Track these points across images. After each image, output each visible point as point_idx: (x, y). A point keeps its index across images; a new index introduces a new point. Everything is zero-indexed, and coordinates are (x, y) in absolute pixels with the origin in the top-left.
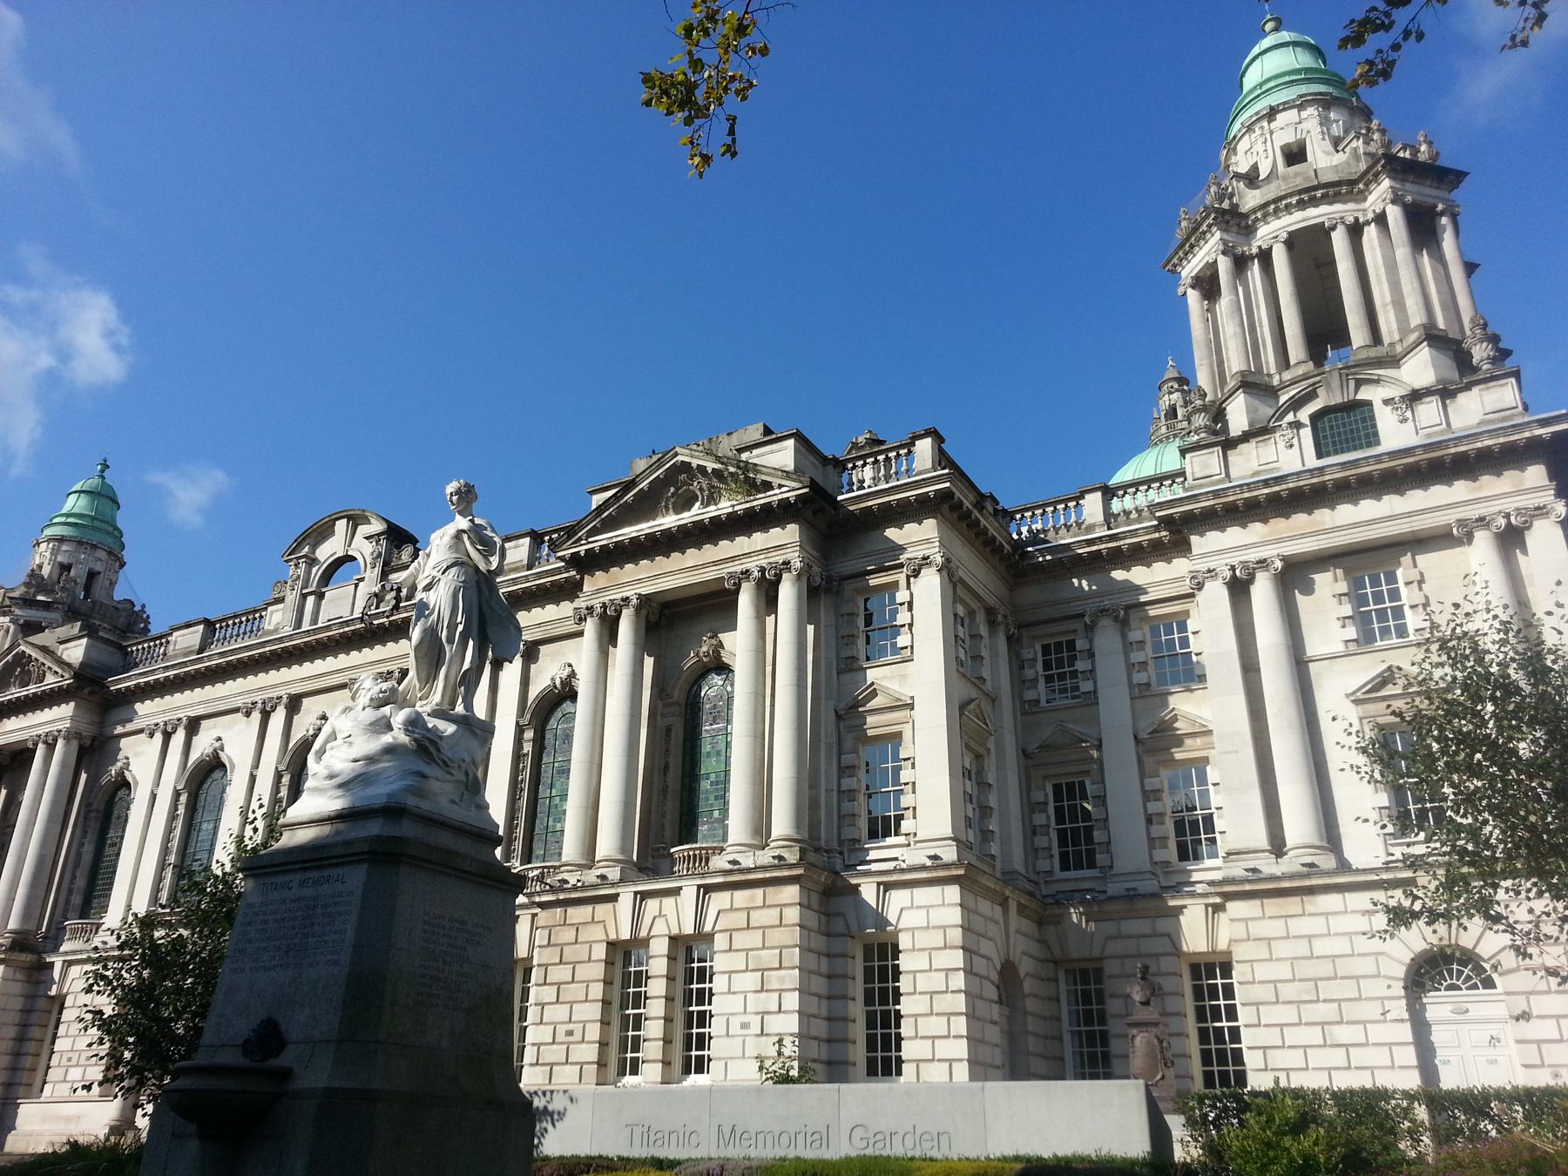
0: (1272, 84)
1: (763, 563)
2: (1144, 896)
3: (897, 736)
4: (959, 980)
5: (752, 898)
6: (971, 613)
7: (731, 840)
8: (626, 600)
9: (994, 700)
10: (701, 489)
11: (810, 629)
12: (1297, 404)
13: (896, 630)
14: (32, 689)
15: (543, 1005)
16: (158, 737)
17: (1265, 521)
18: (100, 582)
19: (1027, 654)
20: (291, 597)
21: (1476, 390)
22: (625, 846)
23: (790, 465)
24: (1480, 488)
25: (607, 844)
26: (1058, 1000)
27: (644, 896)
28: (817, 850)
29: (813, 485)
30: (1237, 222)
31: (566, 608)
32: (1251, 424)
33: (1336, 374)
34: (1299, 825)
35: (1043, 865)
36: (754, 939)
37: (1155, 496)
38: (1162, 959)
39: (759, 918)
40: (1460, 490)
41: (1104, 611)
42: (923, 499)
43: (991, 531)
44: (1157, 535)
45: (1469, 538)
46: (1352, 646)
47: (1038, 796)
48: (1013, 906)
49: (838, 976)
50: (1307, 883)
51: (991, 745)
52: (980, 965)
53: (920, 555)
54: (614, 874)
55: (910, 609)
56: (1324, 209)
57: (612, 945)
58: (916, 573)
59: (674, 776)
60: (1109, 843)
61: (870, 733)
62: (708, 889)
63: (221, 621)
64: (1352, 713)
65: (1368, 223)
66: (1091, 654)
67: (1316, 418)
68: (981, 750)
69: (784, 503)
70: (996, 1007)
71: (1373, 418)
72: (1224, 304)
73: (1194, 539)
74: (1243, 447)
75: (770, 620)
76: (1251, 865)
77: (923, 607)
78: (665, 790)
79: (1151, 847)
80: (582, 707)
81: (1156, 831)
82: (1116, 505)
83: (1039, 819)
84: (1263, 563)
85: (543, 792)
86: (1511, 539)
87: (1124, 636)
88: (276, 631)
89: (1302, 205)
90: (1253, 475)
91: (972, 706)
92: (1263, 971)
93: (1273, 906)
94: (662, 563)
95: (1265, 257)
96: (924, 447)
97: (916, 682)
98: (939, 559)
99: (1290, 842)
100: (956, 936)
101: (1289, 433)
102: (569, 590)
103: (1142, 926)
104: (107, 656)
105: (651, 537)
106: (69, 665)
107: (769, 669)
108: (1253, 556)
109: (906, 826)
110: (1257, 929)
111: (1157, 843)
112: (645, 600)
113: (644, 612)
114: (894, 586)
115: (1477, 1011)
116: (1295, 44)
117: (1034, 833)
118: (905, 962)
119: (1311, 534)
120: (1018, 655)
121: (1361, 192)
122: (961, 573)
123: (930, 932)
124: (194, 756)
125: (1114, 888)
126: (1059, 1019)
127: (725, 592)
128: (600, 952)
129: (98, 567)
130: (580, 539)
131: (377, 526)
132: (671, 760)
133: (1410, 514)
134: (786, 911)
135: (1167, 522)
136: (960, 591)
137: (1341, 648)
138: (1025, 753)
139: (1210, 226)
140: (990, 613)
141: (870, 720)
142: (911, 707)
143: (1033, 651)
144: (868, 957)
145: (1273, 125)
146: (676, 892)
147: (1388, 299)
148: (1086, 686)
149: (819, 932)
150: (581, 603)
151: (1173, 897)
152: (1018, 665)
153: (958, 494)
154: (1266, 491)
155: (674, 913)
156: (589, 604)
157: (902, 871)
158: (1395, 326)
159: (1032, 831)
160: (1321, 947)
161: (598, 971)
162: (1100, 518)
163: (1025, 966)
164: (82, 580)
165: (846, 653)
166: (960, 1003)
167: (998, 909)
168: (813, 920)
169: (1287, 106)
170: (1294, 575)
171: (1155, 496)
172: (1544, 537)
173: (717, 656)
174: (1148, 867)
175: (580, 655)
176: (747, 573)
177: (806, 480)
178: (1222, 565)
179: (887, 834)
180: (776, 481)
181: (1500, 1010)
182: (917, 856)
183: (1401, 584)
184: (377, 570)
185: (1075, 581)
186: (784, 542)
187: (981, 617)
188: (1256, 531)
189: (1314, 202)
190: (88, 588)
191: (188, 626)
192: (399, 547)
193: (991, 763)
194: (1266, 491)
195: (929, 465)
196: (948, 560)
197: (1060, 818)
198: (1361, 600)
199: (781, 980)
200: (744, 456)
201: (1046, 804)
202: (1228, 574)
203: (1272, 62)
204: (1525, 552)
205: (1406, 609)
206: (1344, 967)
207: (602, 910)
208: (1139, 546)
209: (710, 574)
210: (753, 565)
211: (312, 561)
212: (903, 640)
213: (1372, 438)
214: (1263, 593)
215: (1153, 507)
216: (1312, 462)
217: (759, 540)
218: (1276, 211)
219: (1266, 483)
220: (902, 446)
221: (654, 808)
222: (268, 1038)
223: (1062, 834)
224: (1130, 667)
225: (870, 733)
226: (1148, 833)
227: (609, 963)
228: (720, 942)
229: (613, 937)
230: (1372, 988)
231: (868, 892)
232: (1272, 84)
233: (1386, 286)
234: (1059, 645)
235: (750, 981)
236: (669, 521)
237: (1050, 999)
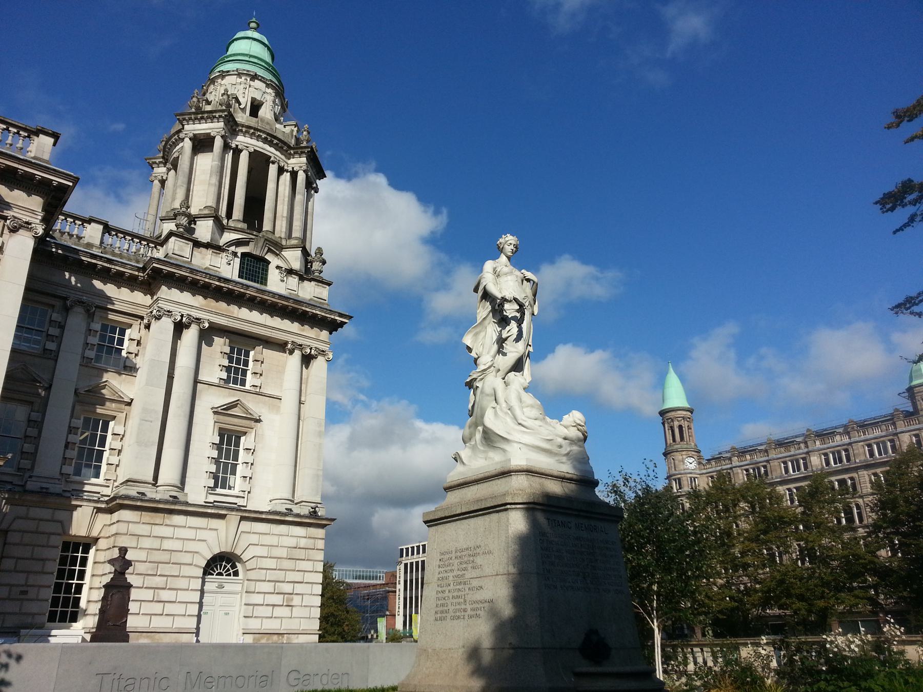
0: (256, 61)
2: (52, 494)
12: (238, 243)
17: (205, 298)
21: (313, 283)
24: (303, 330)
30: (233, 127)
33: (263, 240)
34: (169, 473)
38: (53, 537)
40: (295, 327)
41: (81, 303)
44: (137, 273)
45: (291, 352)
46: (222, 382)
50: (173, 507)
56: (272, 150)
64: (211, 418)
65: (287, 171)
66: (62, 327)
67: (243, 254)
71: (267, 271)
72: (206, 162)
73: (164, 288)
74: (203, 250)
76: (142, 490)
84: (198, 320)
86: (307, 360)
89: (265, 141)
93: (147, 517)
95: (237, 152)
99: (160, 482)
101: (231, 257)
103: (45, 513)
110: (133, 528)
111: (67, 461)
115: (228, 587)
116: (269, 49)
119: (226, 316)
121: (290, 154)
125: (30, 486)
133: (273, 328)
137: (217, 381)
139: (220, 116)
145: (252, 83)
147: (285, 214)
151: (76, 499)
154: (217, 283)
158: (284, 230)
160: (167, 545)
169: (262, 80)
170: (208, 334)
172: (319, 364)
174: (58, 476)
178: (177, 311)
181: (238, 588)
183: (251, 359)
185: (67, 274)
188: (199, 301)
189: (271, 144)
194: (217, 283)
198: (231, 359)
202: (179, 318)
203: (248, 45)
204: (307, 368)
205: (249, 373)
206: (176, 557)
213: (264, 281)
214: (190, 335)
216: (235, 277)
218: (253, 134)
219: (220, 279)
220: (25, 130)
230: (186, 571)
232: (256, 61)
233: (286, 207)
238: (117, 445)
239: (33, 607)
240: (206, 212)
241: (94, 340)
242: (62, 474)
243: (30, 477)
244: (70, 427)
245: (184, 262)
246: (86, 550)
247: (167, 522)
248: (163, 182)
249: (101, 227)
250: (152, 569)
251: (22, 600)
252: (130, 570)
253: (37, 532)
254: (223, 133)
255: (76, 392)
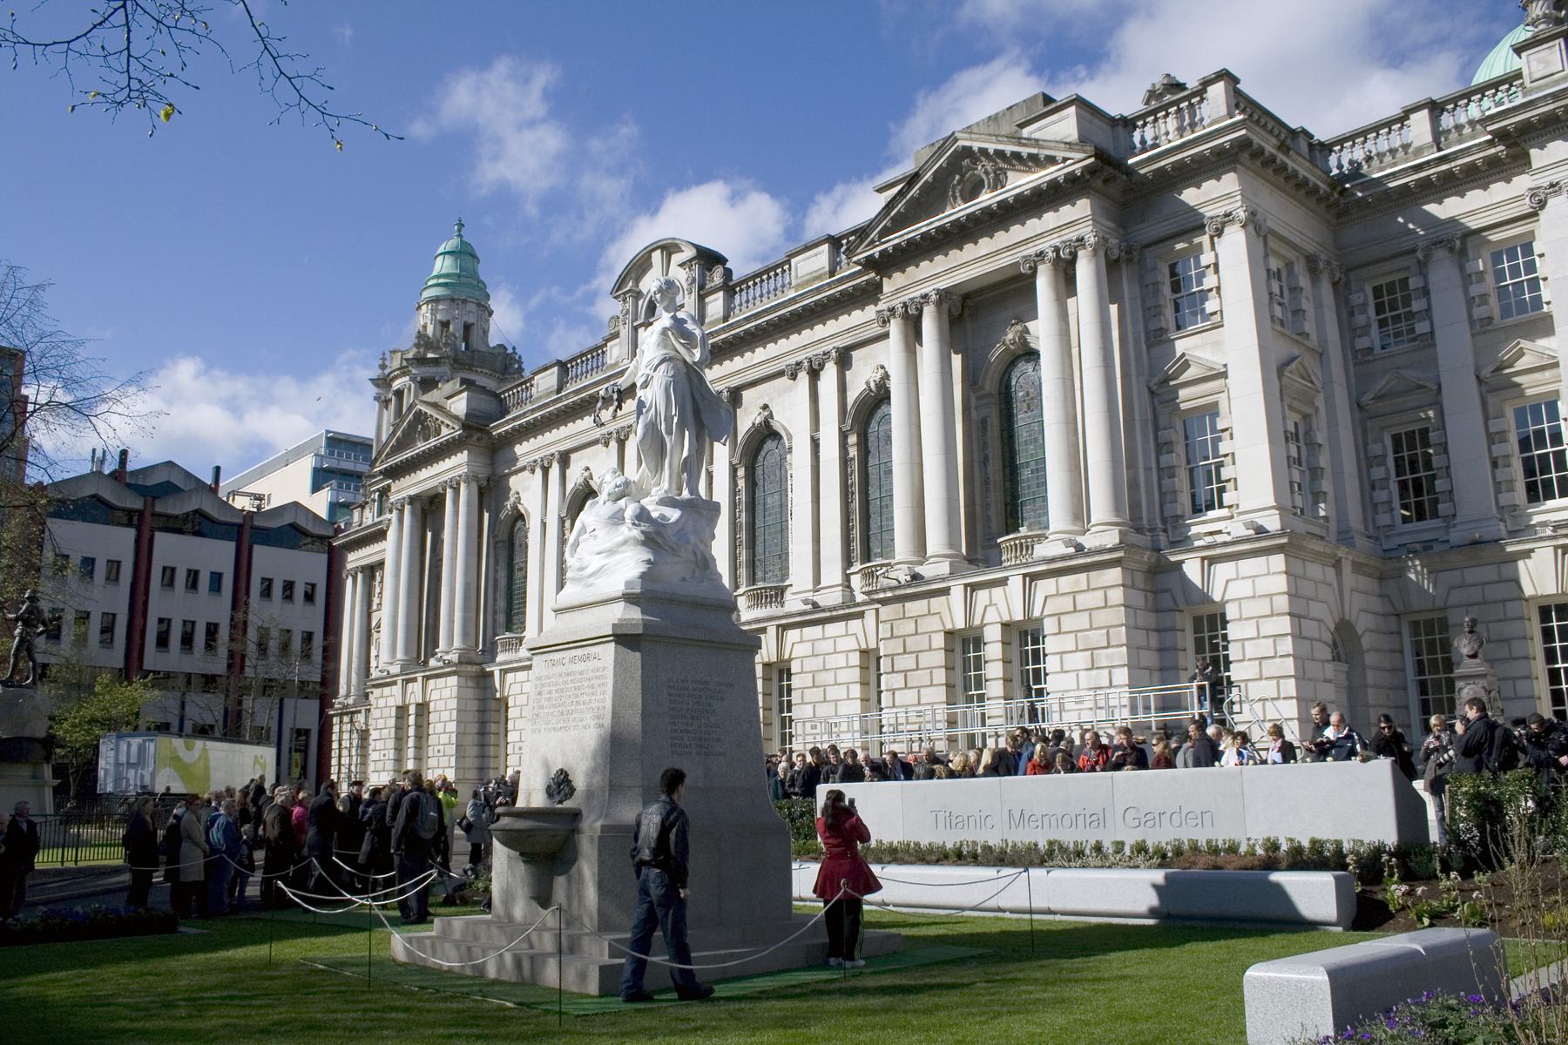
1: (1056, 242)
3: (1212, 410)
4: (1287, 646)
5: (1077, 583)
6: (1289, 265)
7: (1052, 528)
8: (925, 296)
9: (1321, 355)
10: (987, 173)
11: (1114, 308)
13: (1204, 295)
14: (433, 442)
15: (893, 691)
16: (539, 472)
18: (475, 334)
19: (1357, 299)
20: (625, 332)
22: (952, 542)
23: (1073, 135)
25: (935, 540)
26: (1401, 652)
27: (974, 587)
28: (1139, 530)
29: (1100, 155)
31: (870, 312)
35: (1384, 519)
36: (1081, 621)
37: (1489, 106)
39: (1085, 600)
42: (1219, 152)
43: (1302, 172)
44: (1493, 151)
47: (1376, 449)
48: (1347, 567)
49: (1167, 649)
51: (1320, 402)
52: (1310, 628)
53: (1221, 211)
54: (944, 568)
55: (1216, 265)
57: (949, 634)
58: (1219, 233)
59: (995, 468)
60: (1451, 491)
61: (1183, 406)
62: (1034, 577)
63: (570, 361)
66: (1426, 292)
68: (1309, 410)
69: (1071, 179)
70: (1330, 667)
73: (1534, 152)
75: (1071, 302)
77: (1229, 268)
78: (986, 482)
79: (1498, 491)
80: (897, 408)
81: (1501, 474)
82: (1447, 121)
83: (1378, 473)
85: (874, 493)
87: (1462, 268)
88: (616, 364)
91: (1293, 365)
94: (956, 256)
96: (1217, 91)
97: (1229, 350)
98: (1242, 215)
100: (1283, 603)
102: (869, 294)
103: (1489, 573)
104: (486, 404)
105: (941, 230)
106: (456, 418)
107: (1075, 351)
109: (1228, 498)
112: (944, 295)
113: (945, 307)
114: (1199, 249)
117: (1373, 488)
118: (1233, 631)
120: (1347, 301)
122: (1270, 224)
123: (1255, 601)
124: (570, 487)
126: (1403, 670)
127: (1021, 276)
128: (939, 640)
129: (471, 319)
130: (873, 241)
131: (689, 253)
132: (990, 452)
134: (1110, 593)
135: (1501, 136)
136: (1272, 243)
138: (1358, 406)
140: (1312, 263)
141: (1183, 393)
142: (1224, 375)
143: (1364, 296)
144: (1198, 628)
146: (1003, 582)
148: (1422, 327)
149: (1146, 609)
150: (882, 306)
152: (1346, 312)
153: (1256, 140)
155: (1001, 605)
156: (891, 304)
157: (1225, 544)
159: (1370, 486)
161: (939, 658)
162: (1427, 138)
163: (1363, 623)
164: (459, 334)
165: (1153, 326)
166: (1289, 666)
167: (1331, 572)
168: (1139, 598)
171: (1489, 106)
173: (1025, 343)
175: (889, 354)
176: (1041, 255)
177: (1090, 149)
179: (1210, 507)
180: (1059, 155)
182: (1238, 529)
184: (694, 296)
186: (1076, 218)
187: (1300, 267)
190: (466, 338)
191: (546, 369)
192: (710, 270)
193: (1321, 421)
195: (1223, 111)
196: (1253, 214)
197: (1399, 470)
199: (1109, 657)
200: (1026, 132)
201: (1384, 456)
207: (937, 603)
209: (1005, 260)
210: (1046, 245)
211: (638, 295)
212: (1211, 305)
215: (1486, 120)
217: (1050, 219)
221: (978, 502)
222: (561, 784)
223: (1403, 486)
224: (1470, 302)
225: (1183, 406)
226: (1494, 478)
227: (949, 650)
228: (1049, 626)
229: (949, 626)
231: (1192, 569)
234: (1391, 287)
235: (1081, 660)
236: (957, 211)
237: (1392, 651)
245: (1557, 82)
249: (1425, 112)
253: (1485, 603)
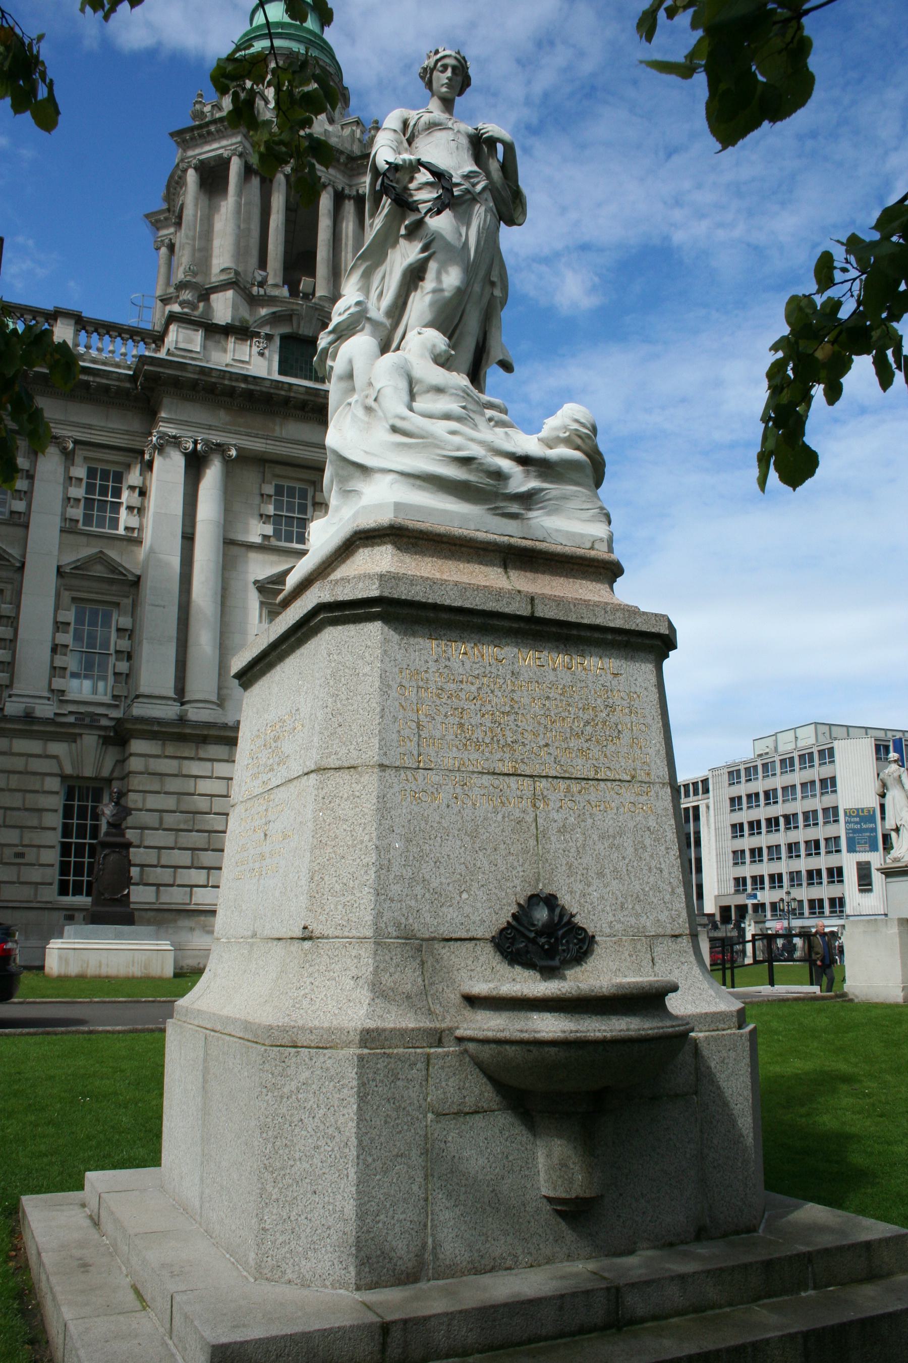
32: (233, 319)
38: (48, 780)
65: (349, 197)
66: (30, 477)
73: (166, 401)
84: (221, 449)
90: (227, 365)
92: (153, 802)
108: (216, 438)
154: (243, 386)
174: (46, 694)
194: (243, 386)
202: (191, 446)
208: (106, 389)
216: (276, 376)
226: (52, 661)
238: (124, 644)
239: (35, 875)
240: (223, 277)
241: (78, 492)
242: (52, 691)
243: (10, 696)
244: (56, 623)
246: (98, 798)
247: (202, 754)
248: (171, 248)
250: (186, 822)
251: (19, 864)
252: (130, 821)
254: (240, 149)
255: (60, 572)
